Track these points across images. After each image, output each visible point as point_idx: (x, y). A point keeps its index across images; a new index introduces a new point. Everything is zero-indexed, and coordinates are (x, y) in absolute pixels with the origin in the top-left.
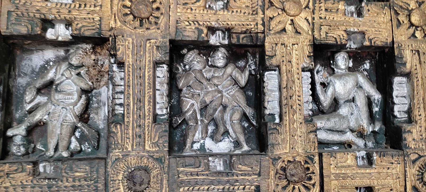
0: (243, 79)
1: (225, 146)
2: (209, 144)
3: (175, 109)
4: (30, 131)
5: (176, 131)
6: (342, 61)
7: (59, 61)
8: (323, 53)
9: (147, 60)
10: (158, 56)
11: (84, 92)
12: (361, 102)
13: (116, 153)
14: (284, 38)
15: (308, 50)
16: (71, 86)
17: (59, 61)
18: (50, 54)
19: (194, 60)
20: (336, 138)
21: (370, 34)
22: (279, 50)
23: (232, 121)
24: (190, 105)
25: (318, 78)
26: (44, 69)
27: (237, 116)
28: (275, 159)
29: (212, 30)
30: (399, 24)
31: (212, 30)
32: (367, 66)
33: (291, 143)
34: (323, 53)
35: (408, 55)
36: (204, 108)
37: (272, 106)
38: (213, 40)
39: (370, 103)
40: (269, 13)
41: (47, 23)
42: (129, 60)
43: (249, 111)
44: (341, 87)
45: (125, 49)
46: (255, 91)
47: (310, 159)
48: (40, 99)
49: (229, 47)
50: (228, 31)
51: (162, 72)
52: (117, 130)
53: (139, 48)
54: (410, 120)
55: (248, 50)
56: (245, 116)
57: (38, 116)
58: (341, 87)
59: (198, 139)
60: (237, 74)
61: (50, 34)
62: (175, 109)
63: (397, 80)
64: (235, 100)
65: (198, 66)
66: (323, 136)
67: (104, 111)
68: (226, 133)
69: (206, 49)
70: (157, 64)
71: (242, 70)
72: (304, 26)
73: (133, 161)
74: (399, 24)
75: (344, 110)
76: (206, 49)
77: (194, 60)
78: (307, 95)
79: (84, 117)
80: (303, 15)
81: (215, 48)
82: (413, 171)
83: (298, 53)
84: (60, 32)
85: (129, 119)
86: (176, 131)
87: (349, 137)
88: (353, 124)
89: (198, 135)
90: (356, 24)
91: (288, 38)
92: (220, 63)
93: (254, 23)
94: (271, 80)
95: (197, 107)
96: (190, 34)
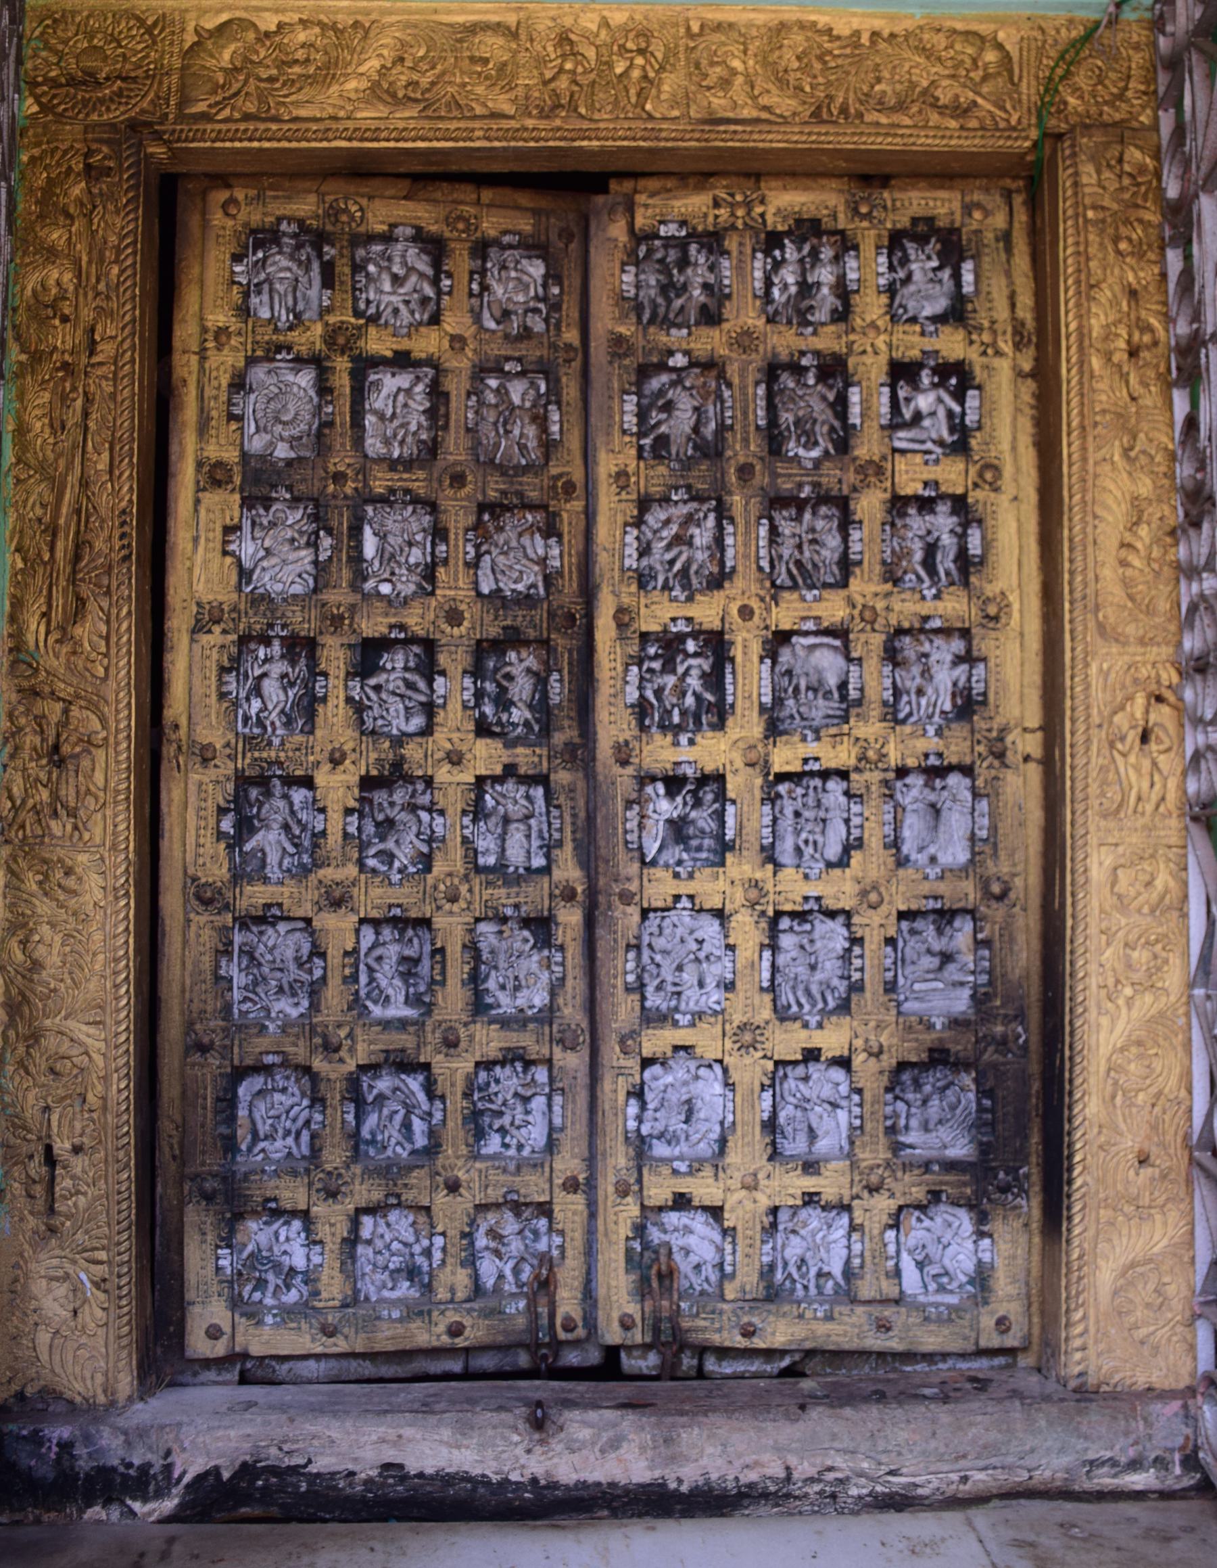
0: (831, 396)
1: (815, 453)
2: (801, 452)
3: (773, 420)
4: (656, 440)
5: (774, 439)
6: (926, 378)
7: (673, 384)
8: (902, 372)
9: (750, 380)
10: (759, 376)
11: (696, 409)
12: (941, 413)
13: (729, 453)
14: (865, 358)
15: (885, 368)
16: (685, 404)
17: (673, 384)
18: (665, 378)
19: (787, 380)
20: (917, 446)
21: (944, 353)
22: (861, 369)
23: (821, 431)
24: (787, 418)
25: (902, 394)
26: (661, 392)
27: (825, 429)
28: (855, 459)
29: (803, 353)
30: (971, 342)
31: (803, 353)
32: (953, 381)
33: (867, 447)
34: (902, 372)
35: (977, 371)
36: (797, 422)
37: (855, 418)
38: (805, 362)
39: (950, 414)
40: (852, 337)
41: (671, 353)
42: (736, 381)
43: (837, 424)
44: (924, 402)
45: (733, 371)
46: (840, 405)
47: (884, 458)
48: (663, 416)
49: (818, 367)
50: (817, 353)
51: (761, 391)
52: (728, 435)
53: (743, 373)
54: (979, 428)
55: (834, 369)
56: (832, 429)
57: (663, 429)
58: (924, 402)
59: (793, 448)
60: (824, 390)
61: (671, 363)
62: (773, 420)
63: (971, 393)
64: (822, 413)
65: (791, 385)
66: (898, 444)
67: (713, 425)
68: (816, 443)
69: (798, 370)
70: (757, 383)
71: (831, 387)
72: (883, 347)
73: (742, 460)
74: (971, 342)
75: (926, 423)
76: (798, 370)
77: (787, 380)
78: (885, 409)
79: (696, 429)
80: (883, 337)
81: (806, 369)
82: (973, 471)
83: (871, 368)
84: (679, 360)
85: (737, 427)
86: (774, 439)
87: (929, 446)
88: (934, 436)
89: (792, 444)
90: (929, 344)
91: (869, 359)
92: (811, 382)
93: (839, 347)
94: (854, 396)
95: (791, 419)
96: (784, 356)
